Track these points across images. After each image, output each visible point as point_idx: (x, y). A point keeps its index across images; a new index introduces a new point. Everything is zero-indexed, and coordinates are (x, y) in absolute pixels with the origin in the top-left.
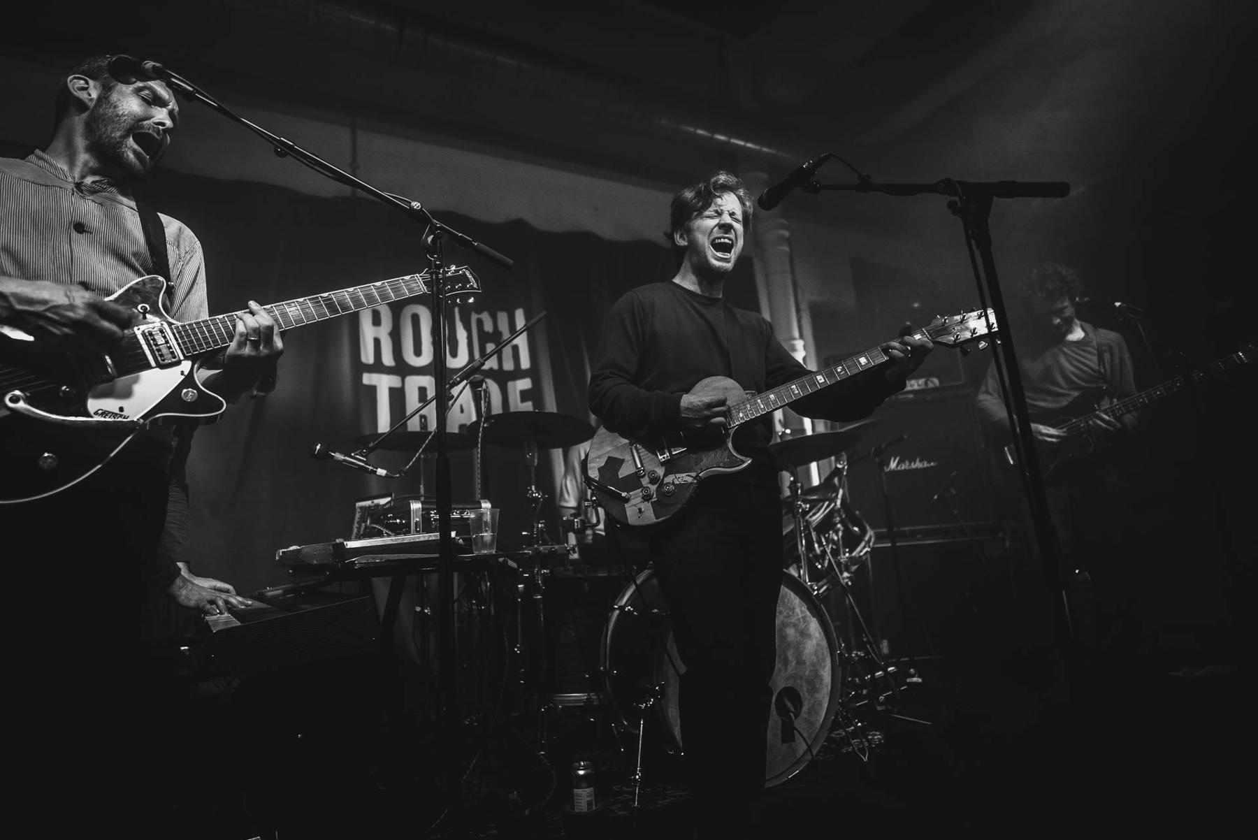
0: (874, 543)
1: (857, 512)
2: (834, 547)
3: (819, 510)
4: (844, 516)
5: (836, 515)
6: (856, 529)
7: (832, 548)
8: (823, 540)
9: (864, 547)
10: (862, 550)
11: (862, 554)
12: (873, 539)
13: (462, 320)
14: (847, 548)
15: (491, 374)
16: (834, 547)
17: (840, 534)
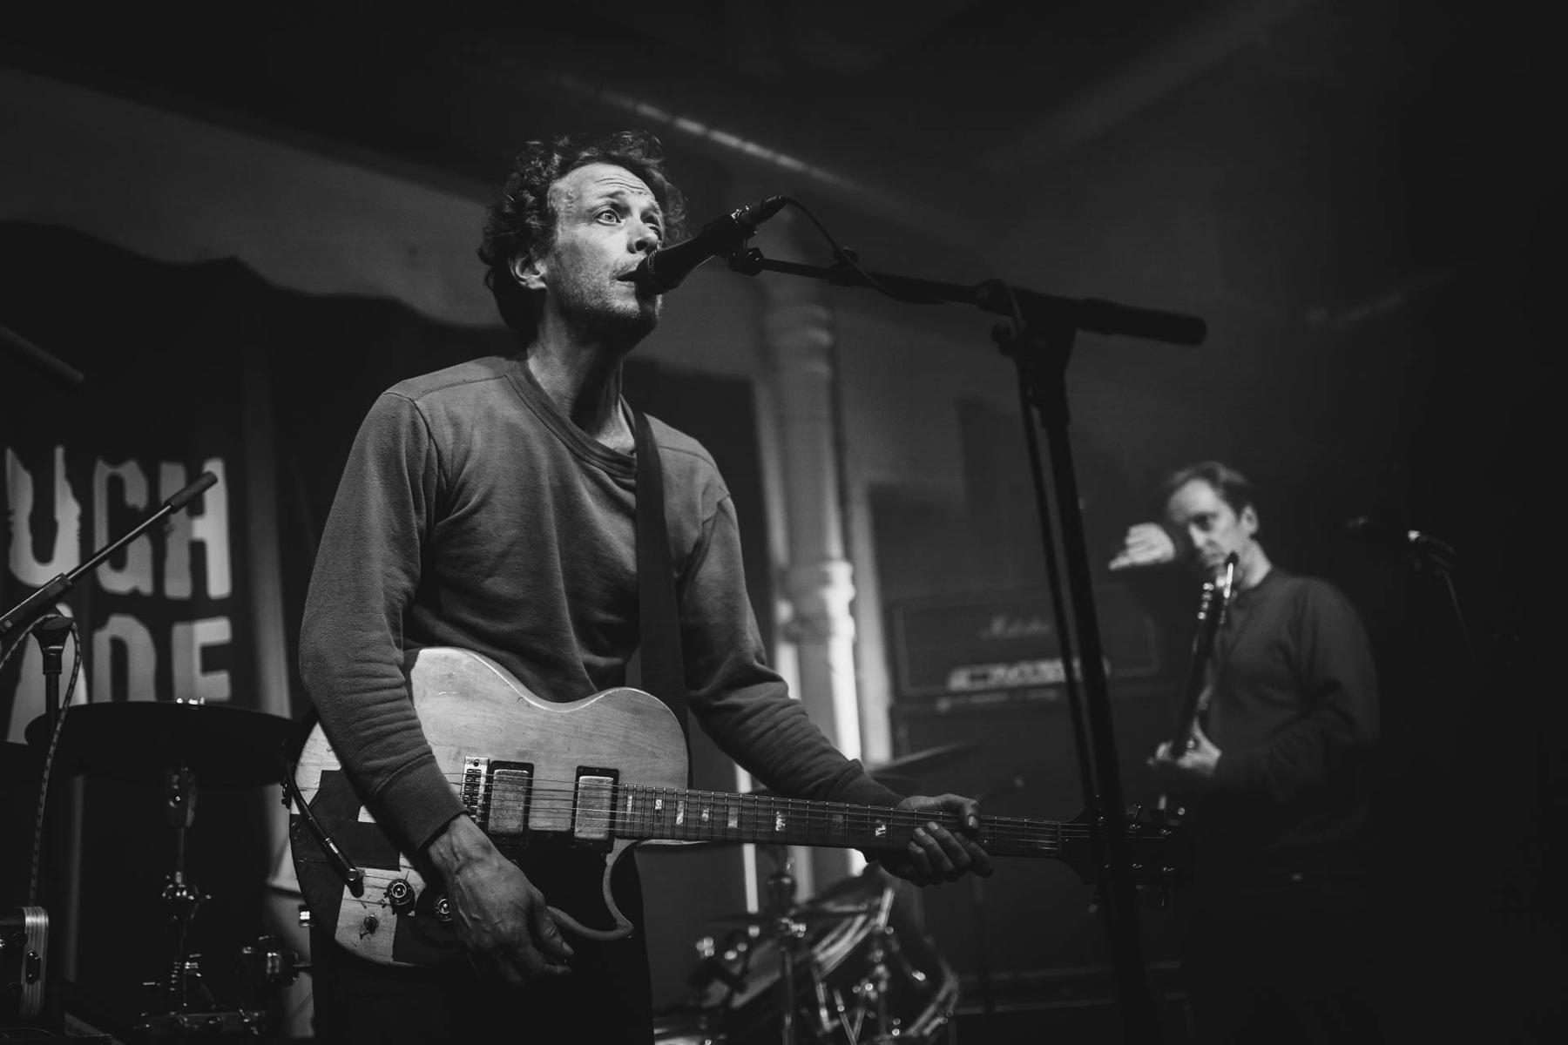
0: (957, 1007)
1: (928, 940)
2: (872, 1015)
3: (843, 933)
4: (895, 948)
5: (875, 944)
6: (920, 976)
7: (866, 1017)
8: (839, 1001)
9: (934, 1016)
10: (929, 1022)
11: (927, 1031)
12: (954, 999)
13: (70, 476)
14: (896, 1017)
15: (130, 604)
16: (872, 1015)
17: (883, 986)
